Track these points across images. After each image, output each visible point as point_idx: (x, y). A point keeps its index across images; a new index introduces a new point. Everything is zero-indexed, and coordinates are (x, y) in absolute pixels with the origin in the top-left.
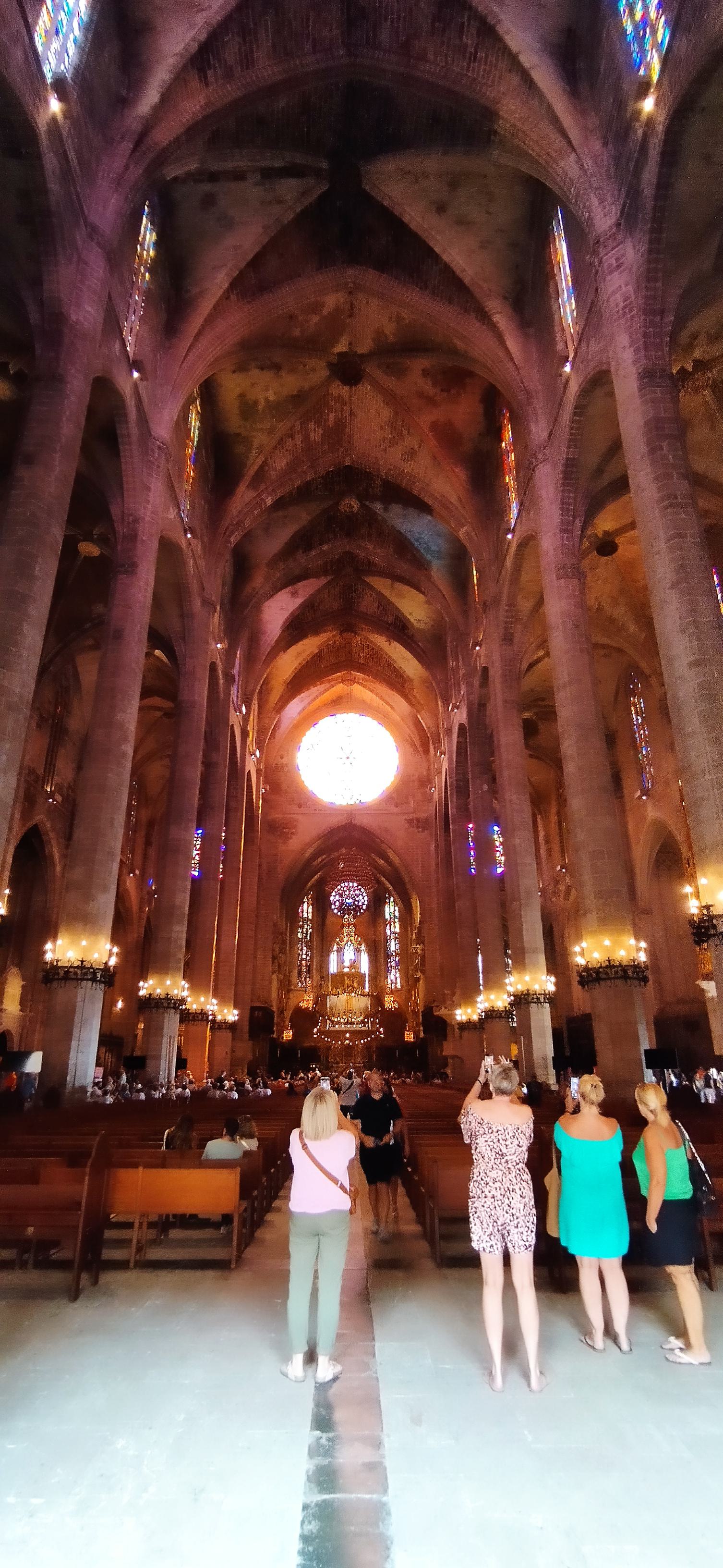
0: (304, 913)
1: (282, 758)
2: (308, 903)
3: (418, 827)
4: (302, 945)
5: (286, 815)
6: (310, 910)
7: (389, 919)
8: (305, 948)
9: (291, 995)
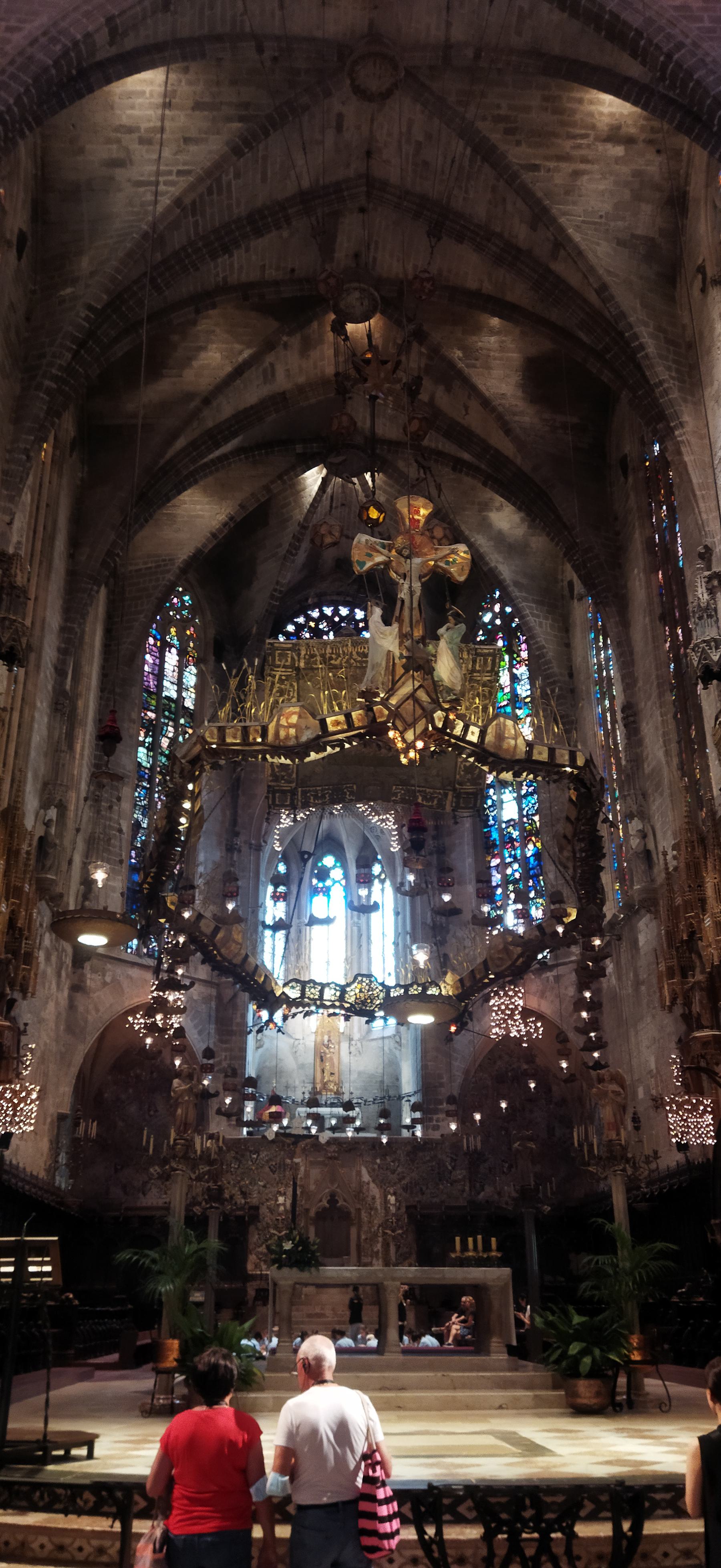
0: (166, 683)
2: (182, 653)
4: (150, 792)
6: (190, 678)
9: (92, 980)
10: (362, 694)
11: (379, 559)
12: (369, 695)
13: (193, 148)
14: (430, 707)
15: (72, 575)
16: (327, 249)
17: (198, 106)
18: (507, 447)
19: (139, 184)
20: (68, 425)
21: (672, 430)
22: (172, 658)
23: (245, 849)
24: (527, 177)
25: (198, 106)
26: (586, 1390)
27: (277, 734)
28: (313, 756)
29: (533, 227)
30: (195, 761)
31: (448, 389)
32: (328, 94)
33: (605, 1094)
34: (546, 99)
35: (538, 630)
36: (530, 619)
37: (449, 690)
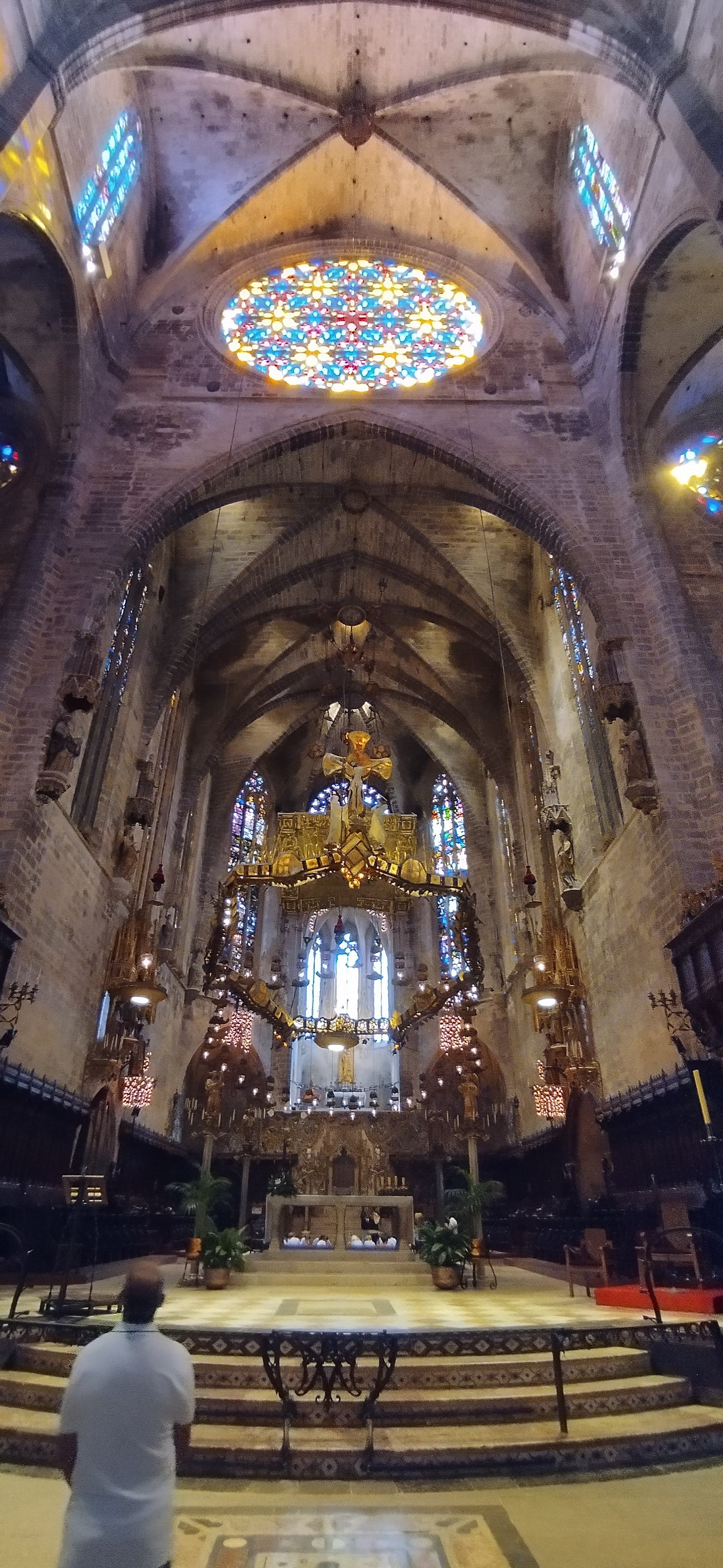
1: (178, 310)
2: (257, 812)
3: (558, 430)
5: (170, 403)
7: (440, 849)
8: (242, 906)
10: (327, 846)
11: (339, 767)
12: (330, 846)
13: (257, 540)
14: (366, 854)
15: (188, 771)
16: (335, 588)
17: (260, 519)
18: (443, 693)
19: (228, 560)
20: (188, 685)
21: (528, 685)
22: (250, 816)
23: (292, 930)
24: (442, 550)
25: (260, 519)
26: (444, 1274)
27: (277, 871)
28: (299, 883)
29: (447, 576)
30: (231, 886)
31: (407, 660)
32: (330, 511)
33: (465, 1089)
34: (450, 510)
35: (467, 797)
36: (462, 789)
37: (378, 844)
